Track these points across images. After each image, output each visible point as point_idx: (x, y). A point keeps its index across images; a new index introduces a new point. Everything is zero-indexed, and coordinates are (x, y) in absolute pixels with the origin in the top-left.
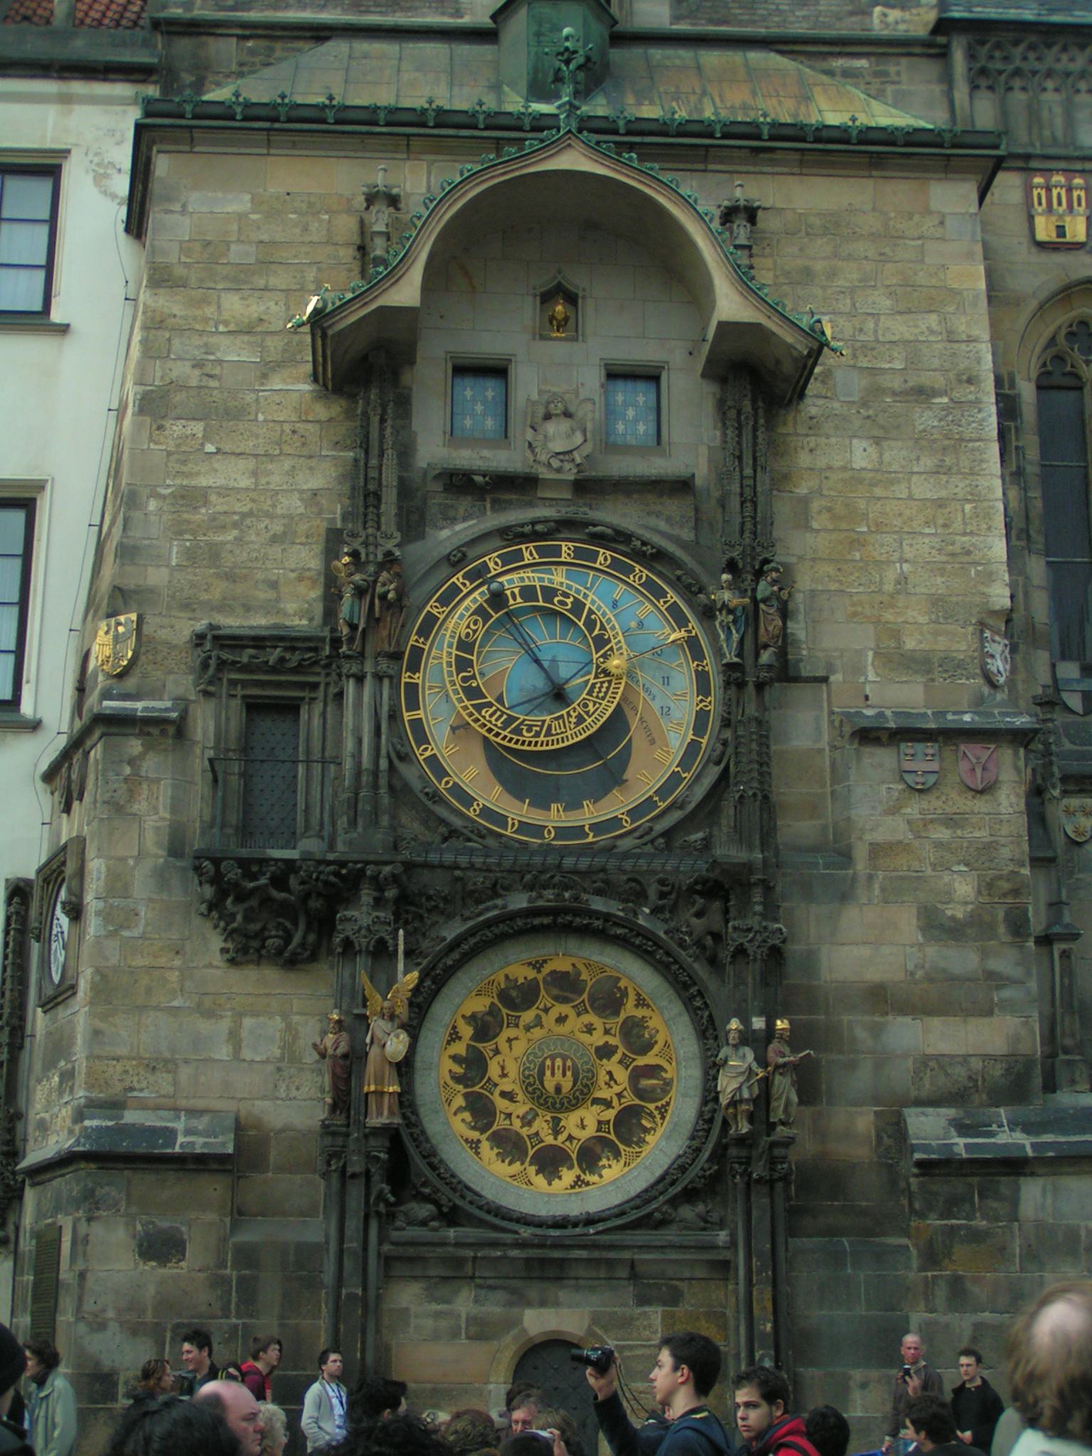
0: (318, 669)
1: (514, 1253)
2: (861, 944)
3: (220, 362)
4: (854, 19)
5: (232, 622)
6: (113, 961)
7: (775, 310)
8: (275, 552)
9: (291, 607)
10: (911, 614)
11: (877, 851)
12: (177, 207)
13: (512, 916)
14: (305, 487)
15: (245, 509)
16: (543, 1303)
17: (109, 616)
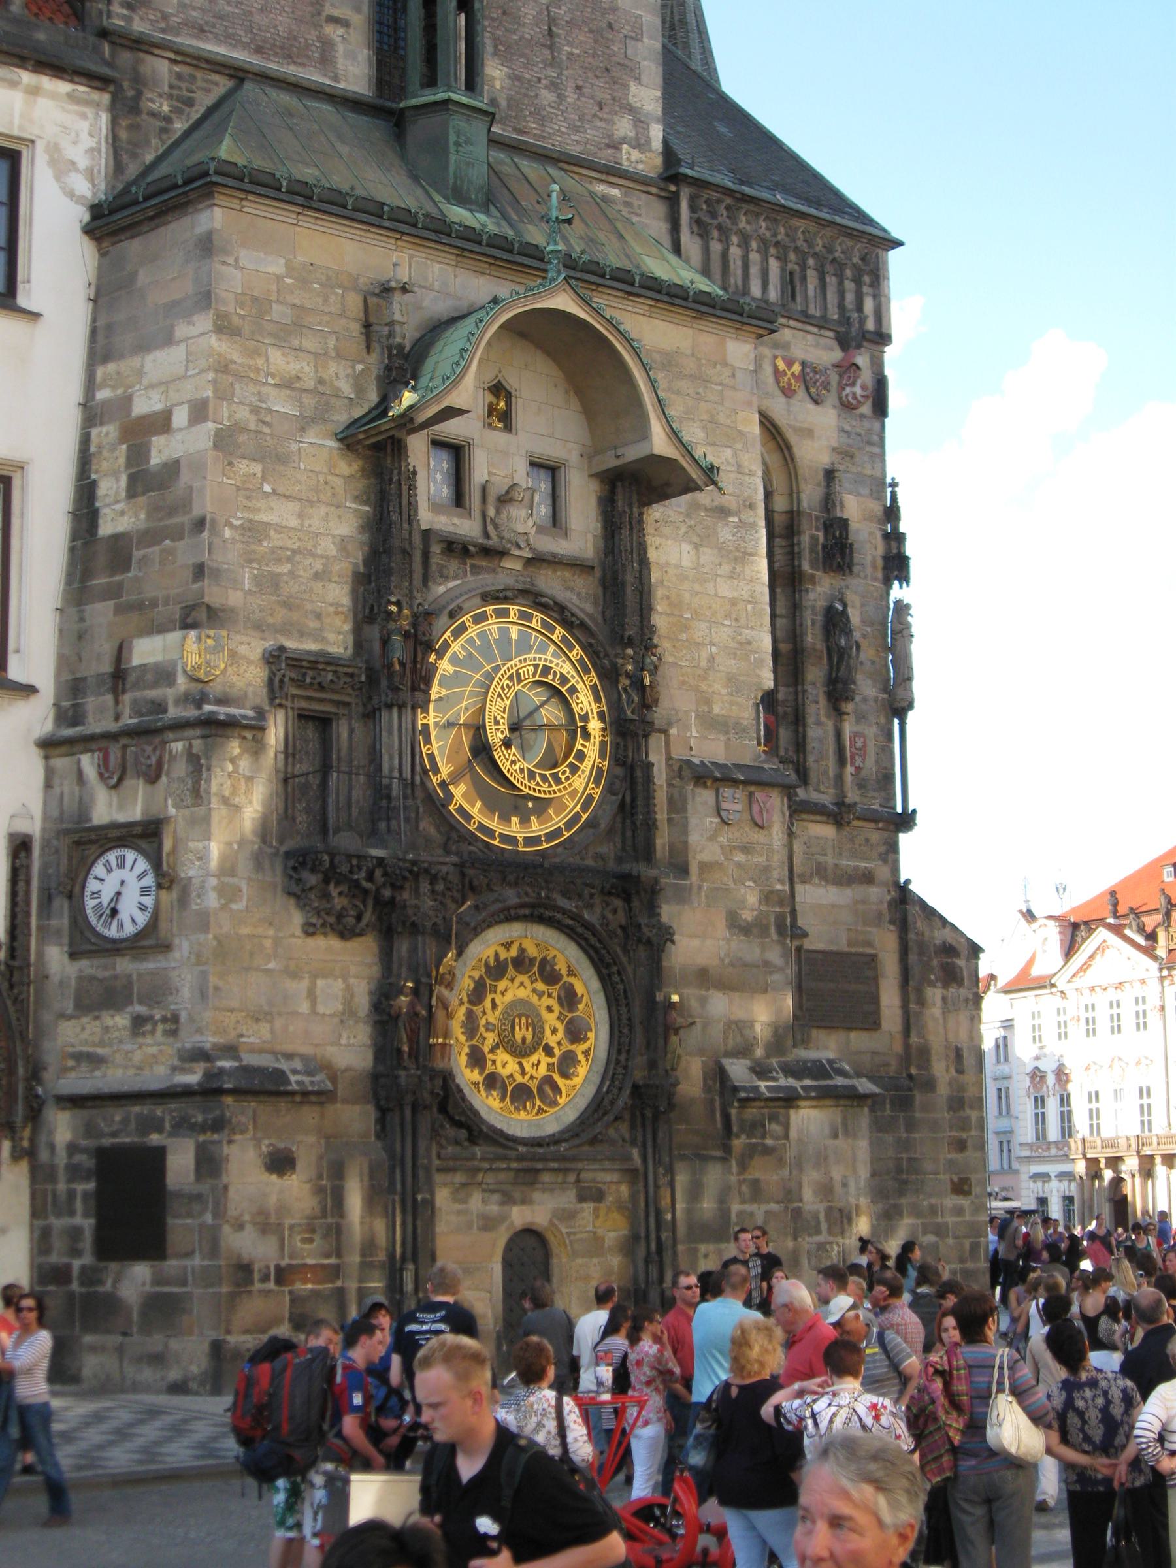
0: (350, 691)
1: (514, 1165)
2: (697, 937)
3: (271, 411)
4: (610, 151)
5: (290, 644)
6: (225, 930)
7: (686, 449)
8: (318, 586)
9: (332, 637)
10: (717, 687)
11: (705, 867)
12: (231, 261)
13: (508, 909)
14: (337, 532)
15: (295, 547)
16: (524, 1202)
17: (187, 625)
